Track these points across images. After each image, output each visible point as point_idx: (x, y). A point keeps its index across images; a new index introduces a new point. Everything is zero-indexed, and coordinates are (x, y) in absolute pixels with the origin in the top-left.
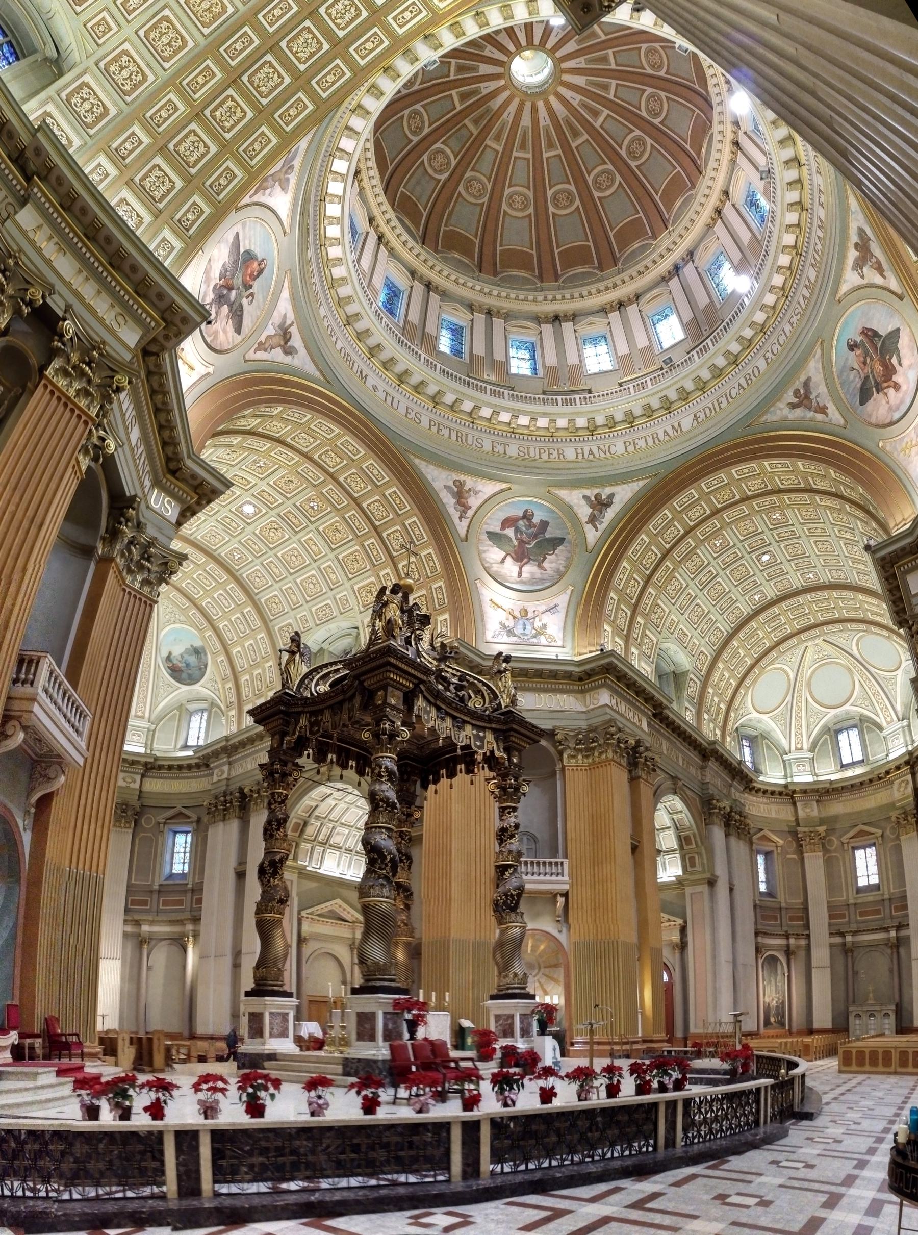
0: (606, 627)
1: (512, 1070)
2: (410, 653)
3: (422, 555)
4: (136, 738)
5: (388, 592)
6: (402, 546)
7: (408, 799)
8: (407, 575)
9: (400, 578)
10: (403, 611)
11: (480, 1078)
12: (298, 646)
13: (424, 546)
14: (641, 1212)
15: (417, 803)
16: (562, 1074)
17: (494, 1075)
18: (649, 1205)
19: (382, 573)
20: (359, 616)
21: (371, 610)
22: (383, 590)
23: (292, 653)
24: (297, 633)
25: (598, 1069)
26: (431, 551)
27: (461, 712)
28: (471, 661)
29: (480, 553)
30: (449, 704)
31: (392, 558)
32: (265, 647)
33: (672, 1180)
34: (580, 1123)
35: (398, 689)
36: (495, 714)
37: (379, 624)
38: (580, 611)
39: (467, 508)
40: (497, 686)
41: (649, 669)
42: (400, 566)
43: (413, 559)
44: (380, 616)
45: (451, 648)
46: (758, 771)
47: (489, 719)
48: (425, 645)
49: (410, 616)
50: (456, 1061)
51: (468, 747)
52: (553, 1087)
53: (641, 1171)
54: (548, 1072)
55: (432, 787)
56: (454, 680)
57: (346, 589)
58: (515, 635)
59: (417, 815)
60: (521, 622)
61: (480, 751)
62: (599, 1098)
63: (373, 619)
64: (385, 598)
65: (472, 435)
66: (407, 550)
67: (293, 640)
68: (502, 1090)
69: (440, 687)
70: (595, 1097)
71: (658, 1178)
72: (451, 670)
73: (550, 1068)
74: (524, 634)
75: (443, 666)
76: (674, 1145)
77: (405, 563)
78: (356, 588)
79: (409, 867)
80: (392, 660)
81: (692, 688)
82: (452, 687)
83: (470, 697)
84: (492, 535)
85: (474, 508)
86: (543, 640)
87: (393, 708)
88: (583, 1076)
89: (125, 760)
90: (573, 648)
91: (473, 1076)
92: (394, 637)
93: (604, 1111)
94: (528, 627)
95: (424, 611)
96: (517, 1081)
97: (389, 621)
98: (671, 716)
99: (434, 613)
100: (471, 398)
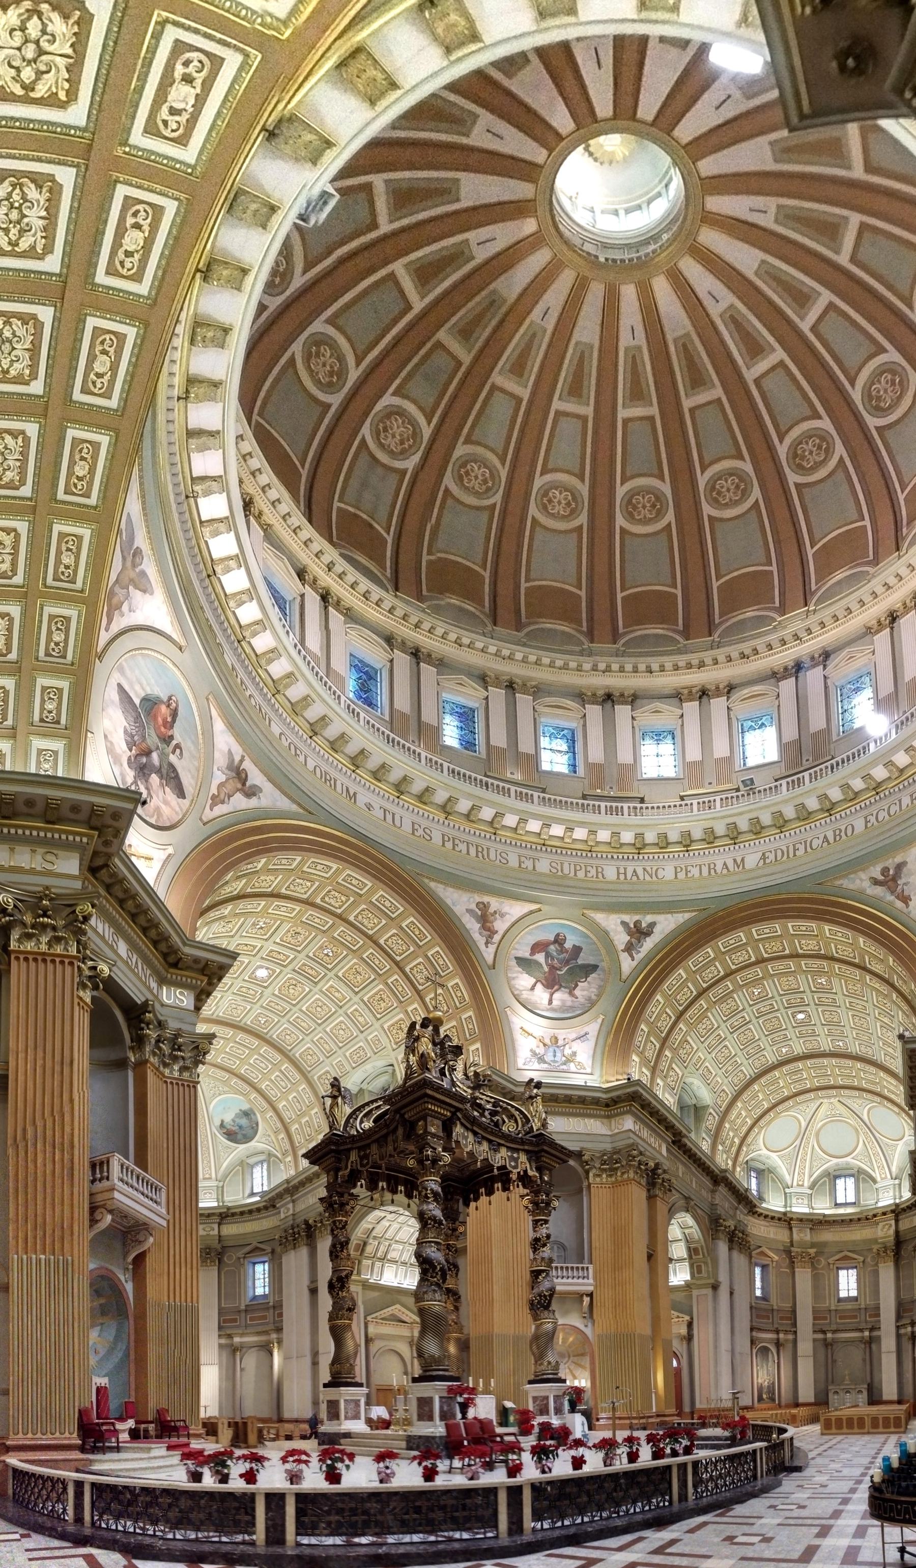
0: (635, 1057)
1: (548, 1443)
2: (445, 1084)
3: (450, 985)
4: (208, 1196)
5: (418, 1027)
6: (428, 979)
7: (452, 1216)
8: (436, 1008)
9: (429, 1011)
10: (435, 1044)
11: (521, 1450)
12: (339, 1090)
13: (451, 976)
14: (662, 1557)
15: (461, 1219)
16: (591, 1444)
17: (533, 1447)
18: (668, 1550)
19: (410, 1009)
20: (393, 1054)
21: (403, 1047)
22: (413, 1025)
23: (334, 1097)
24: (335, 1079)
25: (619, 1439)
26: (457, 980)
27: (496, 1136)
28: (504, 1088)
29: (509, 980)
30: (485, 1129)
31: (418, 992)
32: (308, 1096)
33: (686, 1528)
34: (606, 1485)
35: (437, 1118)
36: (527, 1137)
37: (413, 1059)
38: (610, 1041)
39: (493, 932)
40: (529, 1111)
41: (672, 1100)
42: (427, 1000)
43: (440, 991)
44: (413, 1051)
45: (484, 1076)
46: (761, 1199)
47: (522, 1142)
48: (459, 1075)
49: (442, 1049)
50: (501, 1436)
51: (504, 1167)
52: (583, 1456)
53: (660, 1522)
54: (579, 1443)
55: (473, 1205)
56: (489, 1106)
57: (376, 1030)
58: (545, 1062)
59: (461, 1229)
60: (551, 1049)
61: (515, 1171)
62: (621, 1464)
63: (407, 1055)
64: (416, 1033)
65: (494, 848)
66: (433, 982)
67: (333, 1085)
68: (540, 1460)
69: (476, 1113)
70: (618, 1463)
71: (675, 1527)
72: (485, 1098)
73: (580, 1440)
74: (555, 1061)
75: (477, 1094)
76: (686, 1499)
77: (432, 995)
78: (386, 1026)
79: (457, 1274)
80: (429, 1092)
81: (711, 1122)
82: (487, 1113)
83: (504, 1122)
84: (521, 961)
85: (501, 933)
86: (572, 1067)
87: (434, 1135)
88: (607, 1445)
89: (201, 1215)
90: (601, 1076)
91: (515, 1448)
92: (428, 1069)
93: (626, 1474)
94: (559, 1054)
95: (455, 1042)
96: (552, 1452)
97: (423, 1055)
98: (689, 1144)
99: (465, 1043)
100: (491, 804)
